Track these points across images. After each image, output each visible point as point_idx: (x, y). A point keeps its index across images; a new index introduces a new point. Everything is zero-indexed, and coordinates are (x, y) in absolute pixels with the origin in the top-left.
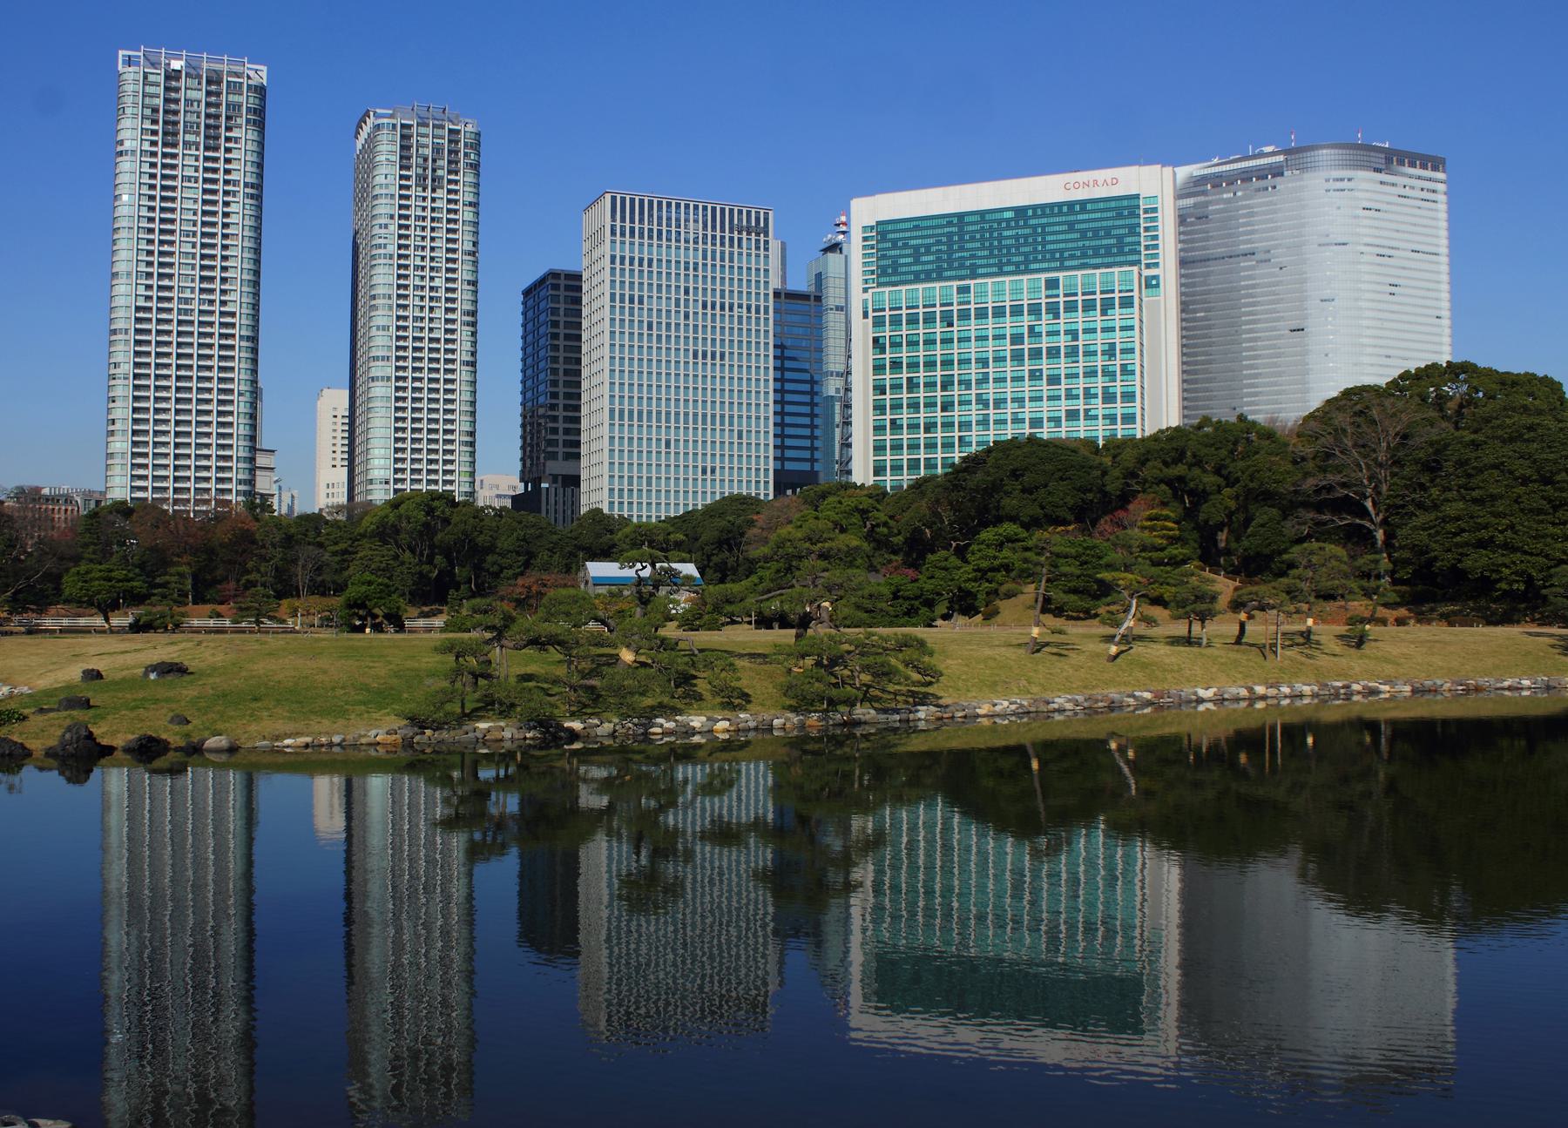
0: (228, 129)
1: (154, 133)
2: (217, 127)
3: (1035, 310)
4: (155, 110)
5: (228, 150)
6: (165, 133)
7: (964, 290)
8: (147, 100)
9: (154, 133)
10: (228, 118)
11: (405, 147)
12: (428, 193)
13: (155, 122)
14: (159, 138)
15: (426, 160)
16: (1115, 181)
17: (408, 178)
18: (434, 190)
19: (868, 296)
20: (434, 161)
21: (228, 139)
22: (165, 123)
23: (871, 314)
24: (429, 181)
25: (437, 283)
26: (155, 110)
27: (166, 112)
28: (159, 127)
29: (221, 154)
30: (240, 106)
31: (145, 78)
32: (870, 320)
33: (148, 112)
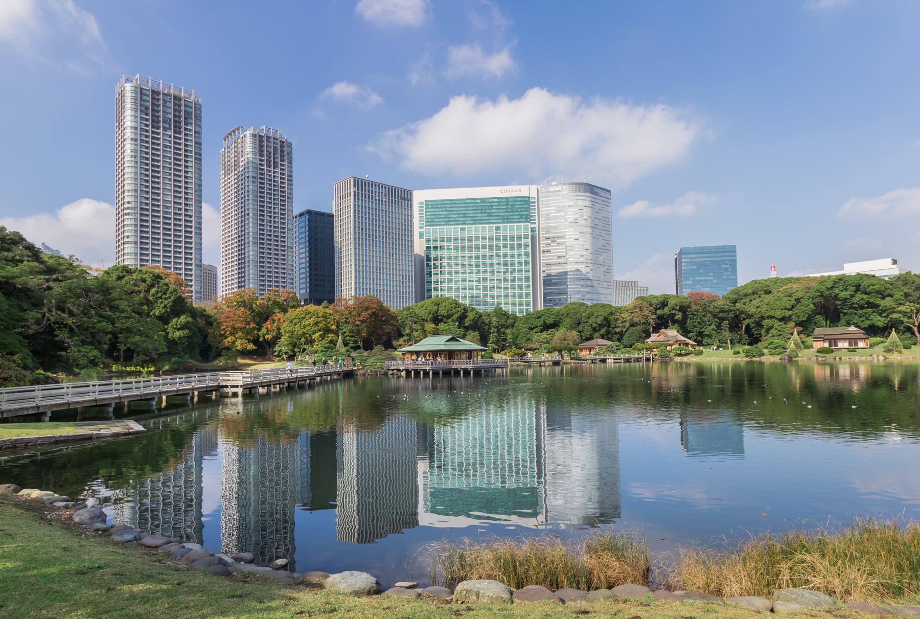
2: (180, 123)
4: (147, 109)
6: (153, 121)
8: (143, 103)
9: (147, 120)
10: (185, 118)
11: (261, 146)
12: (272, 169)
13: (147, 114)
14: (150, 123)
16: (520, 191)
17: (262, 161)
19: (423, 230)
21: (186, 129)
22: (153, 116)
24: (272, 163)
25: (276, 210)
27: (153, 110)
28: (150, 117)
29: (182, 136)
33: (143, 109)
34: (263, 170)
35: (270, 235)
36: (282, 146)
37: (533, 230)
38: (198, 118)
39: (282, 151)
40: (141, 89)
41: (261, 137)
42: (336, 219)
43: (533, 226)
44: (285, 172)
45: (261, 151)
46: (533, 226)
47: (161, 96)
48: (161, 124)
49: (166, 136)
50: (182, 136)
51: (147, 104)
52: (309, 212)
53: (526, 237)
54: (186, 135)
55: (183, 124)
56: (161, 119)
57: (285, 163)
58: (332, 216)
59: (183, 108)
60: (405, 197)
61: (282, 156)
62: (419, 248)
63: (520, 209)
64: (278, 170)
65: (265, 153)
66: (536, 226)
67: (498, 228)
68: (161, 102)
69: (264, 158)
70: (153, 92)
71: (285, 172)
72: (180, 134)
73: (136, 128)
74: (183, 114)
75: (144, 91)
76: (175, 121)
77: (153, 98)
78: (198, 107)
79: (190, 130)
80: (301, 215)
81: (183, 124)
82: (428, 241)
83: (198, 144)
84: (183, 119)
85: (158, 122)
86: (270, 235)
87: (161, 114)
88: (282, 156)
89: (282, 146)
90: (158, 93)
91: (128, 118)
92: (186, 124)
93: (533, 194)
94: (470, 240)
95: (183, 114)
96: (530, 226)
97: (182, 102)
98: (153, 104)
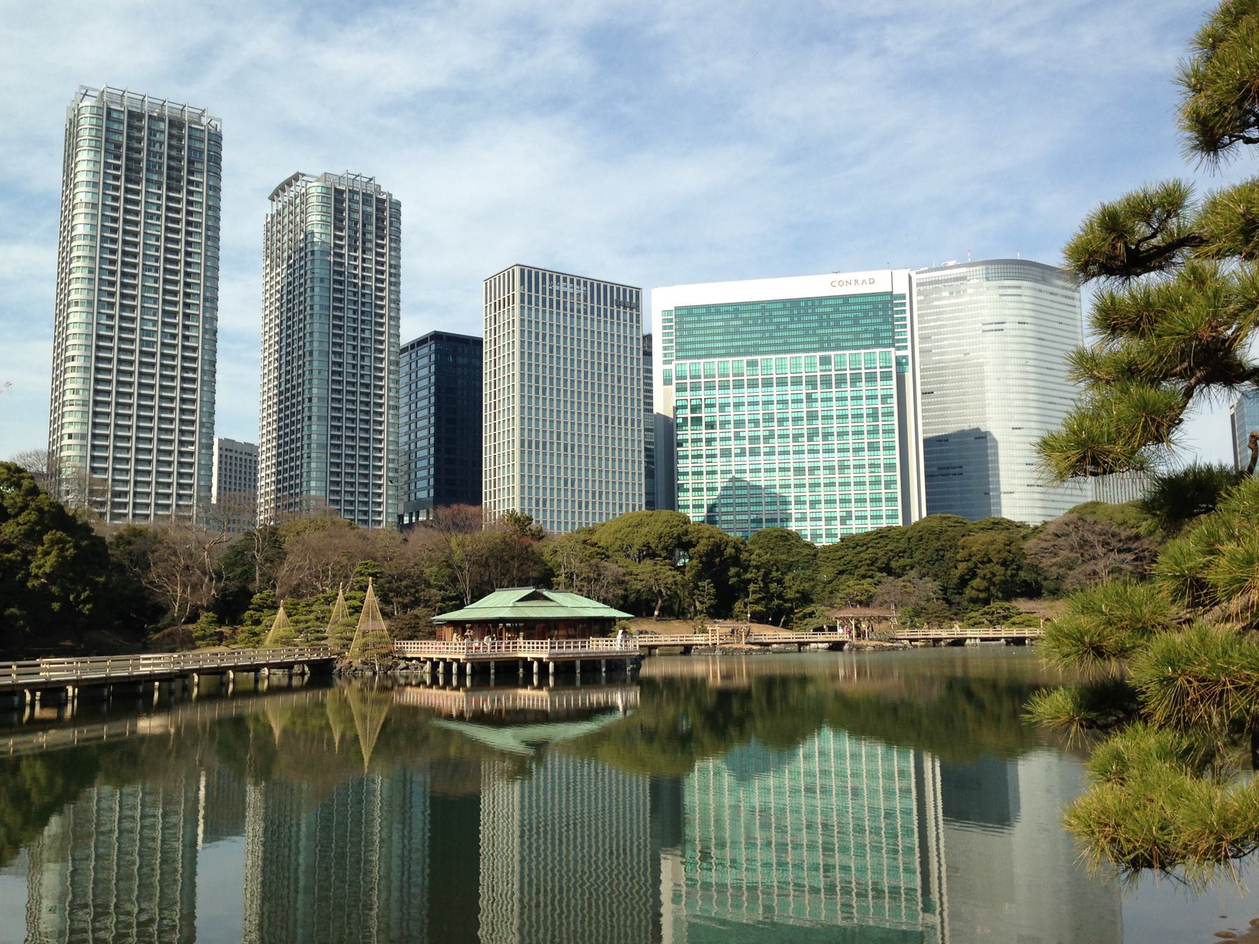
0: (191, 173)
3: (812, 382)
4: (118, 146)
6: (128, 169)
7: (752, 364)
9: (117, 168)
10: (191, 162)
11: (339, 211)
12: (359, 253)
13: (118, 157)
16: (872, 282)
17: (341, 238)
18: (364, 252)
19: (672, 367)
20: (364, 225)
21: (190, 182)
22: (128, 159)
23: (674, 382)
24: (359, 243)
26: (118, 146)
27: (129, 148)
28: (122, 162)
29: (183, 195)
30: (202, 152)
31: (109, 114)
32: (673, 387)
34: (341, 256)
35: (353, 384)
36: (380, 210)
37: (900, 363)
38: (216, 159)
39: (380, 220)
40: (109, 111)
41: (339, 192)
42: (486, 348)
43: (900, 353)
44: (386, 259)
45: (339, 220)
46: (900, 353)
47: (145, 123)
48: (143, 175)
49: (151, 196)
50: (183, 195)
51: (116, 137)
52: (437, 337)
53: (886, 377)
54: (190, 193)
55: (184, 173)
56: (144, 165)
57: (386, 241)
58: (478, 343)
59: (185, 142)
60: (627, 301)
61: (380, 228)
62: (663, 402)
63: (877, 317)
64: (371, 256)
65: (346, 223)
66: (908, 352)
67: (825, 361)
68: (145, 133)
70: (131, 114)
71: (386, 259)
72: (179, 191)
73: (95, 184)
74: (185, 153)
75: (115, 115)
77: (130, 126)
78: (216, 139)
79: (198, 184)
80: (422, 342)
81: (184, 173)
82: (681, 389)
83: (214, 209)
84: (185, 163)
85: (139, 171)
86: (353, 384)
87: (144, 155)
88: (380, 228)
89: (380, 210)
90: (140, 117)
91: (82, 166)
92: (191, 173)
93: (901, 288)
95: (185, 153)
96: (894, 353)
97: (186, 132)
98: (129, 138)
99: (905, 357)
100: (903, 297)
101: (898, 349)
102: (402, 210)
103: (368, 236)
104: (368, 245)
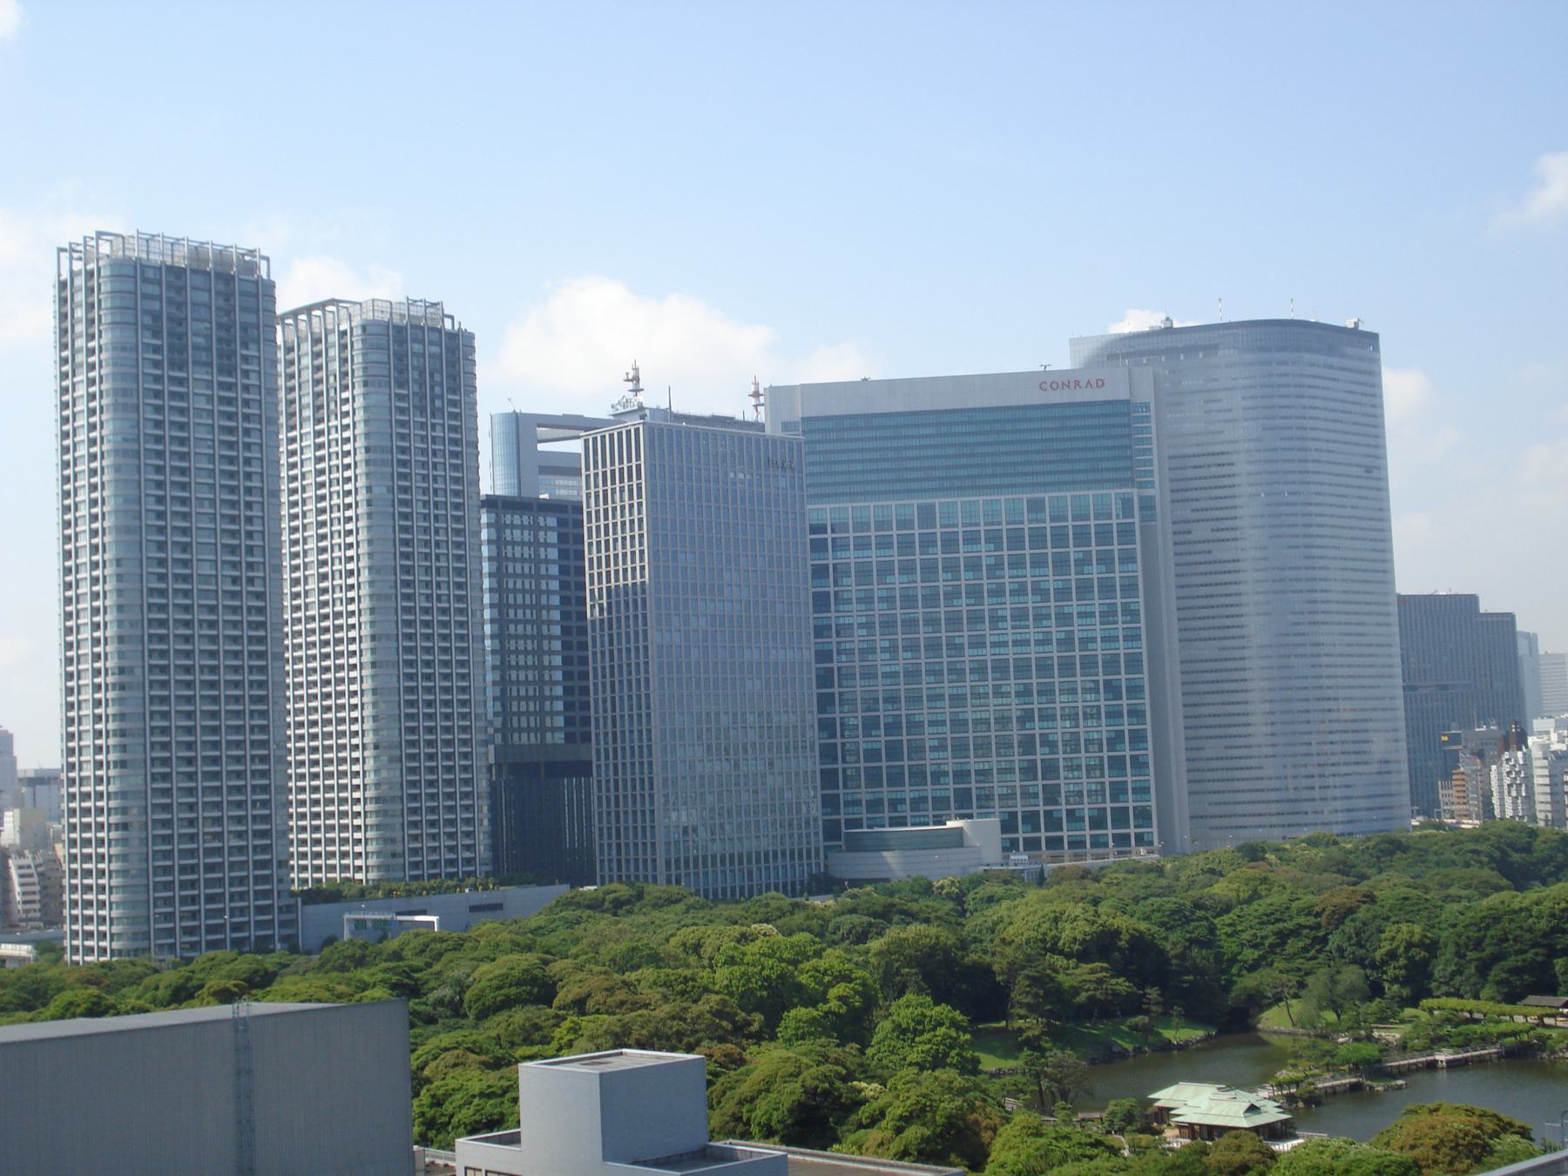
0: (245, 345)
1: (157, 349)
4: (157, 317)
5: (246, 374)
9: (157, 349)
11: (401, 357)
13: (157, 334)
15: (422, 372)
18: (433, 416)
20: (432, 375)
21: (246, 359)
22: (171, 334)
33: (148, 320)
39: (453, 364)
69: (413, 388)
76: (220, 340)
94: (950, 543)
99: (1152, 498)
100: (1147, 407)
101: (1141, 486)
102: (477, 344)
103: (437, 390)
104: (438, 403)
